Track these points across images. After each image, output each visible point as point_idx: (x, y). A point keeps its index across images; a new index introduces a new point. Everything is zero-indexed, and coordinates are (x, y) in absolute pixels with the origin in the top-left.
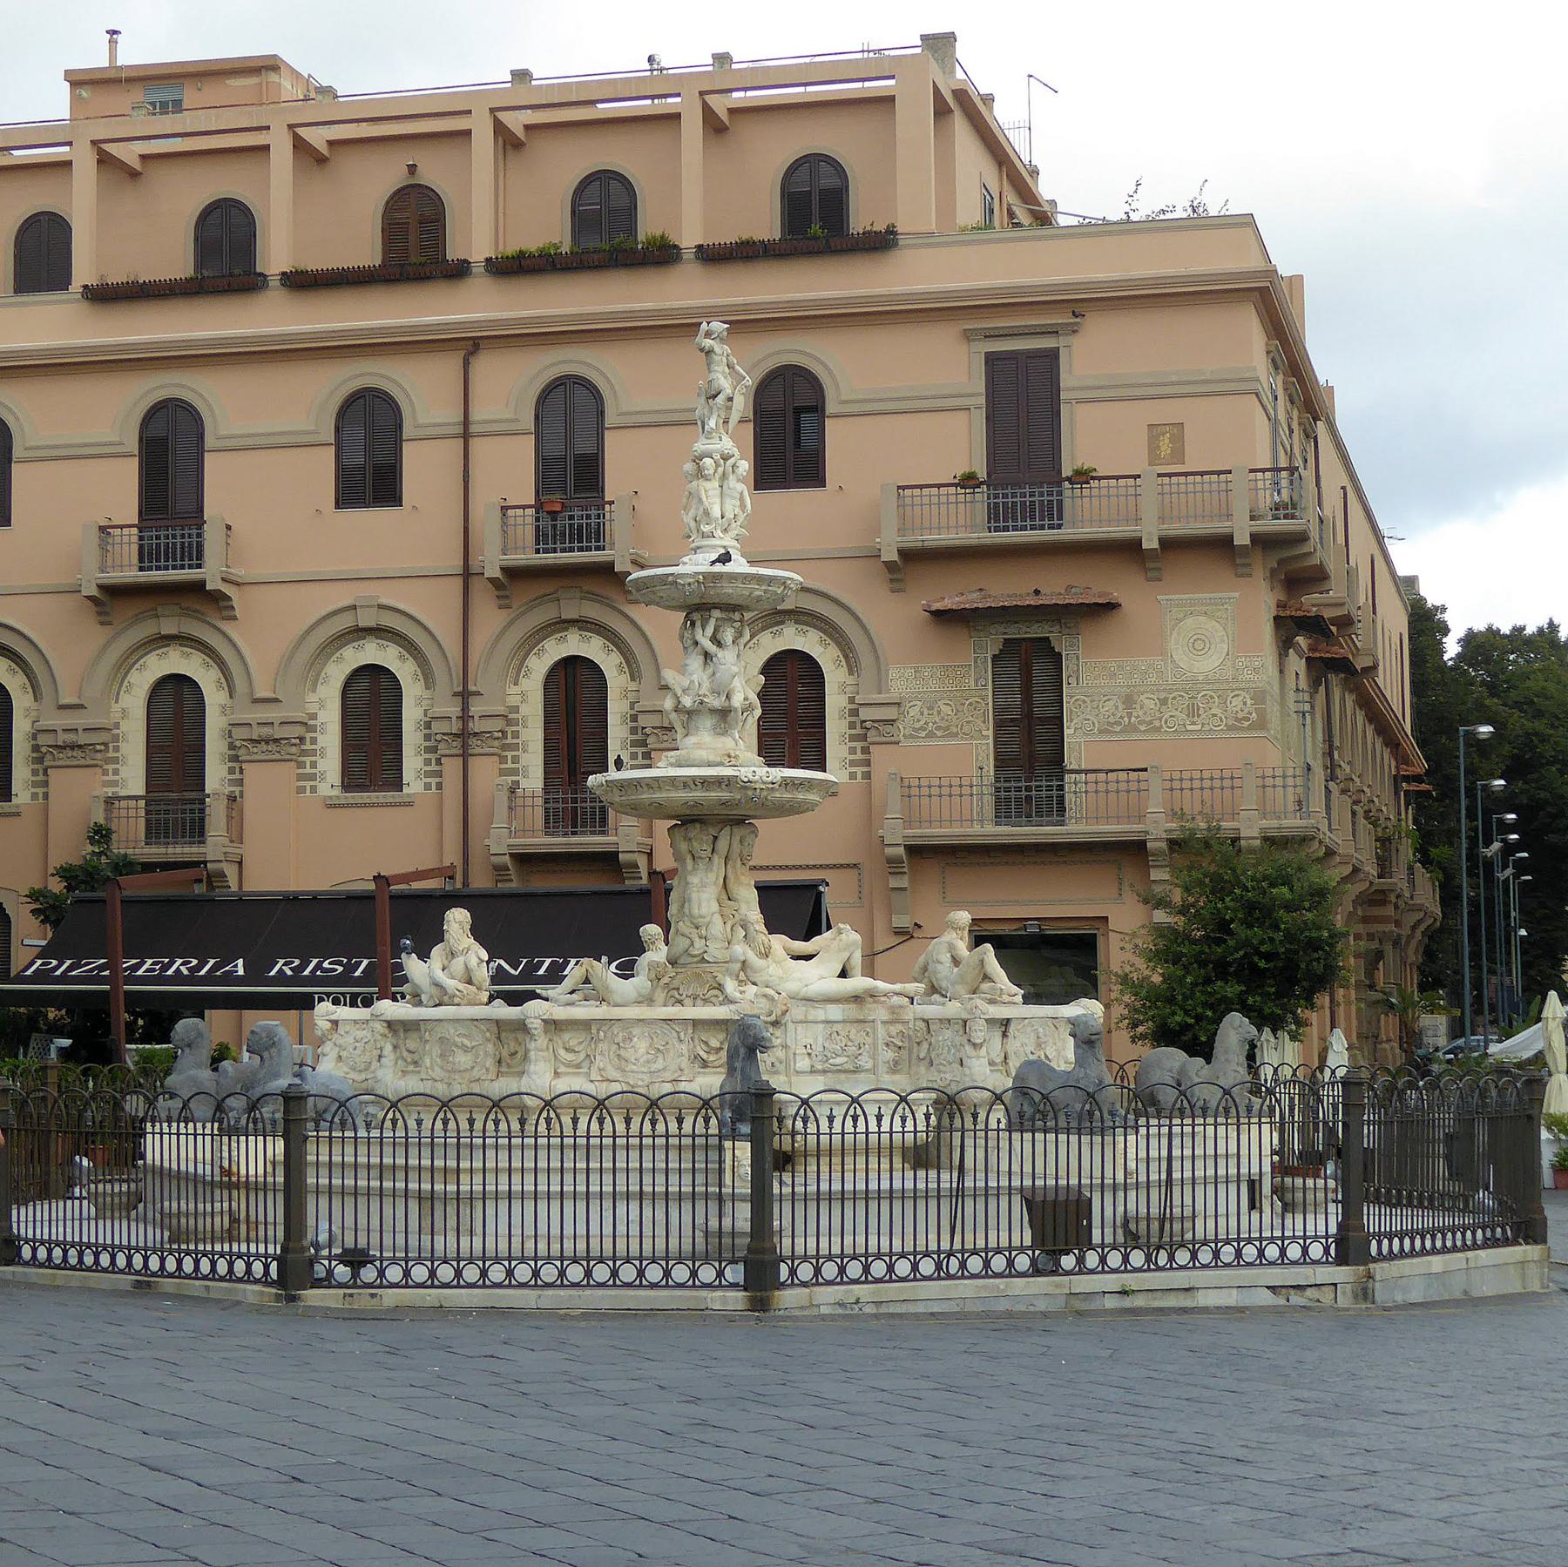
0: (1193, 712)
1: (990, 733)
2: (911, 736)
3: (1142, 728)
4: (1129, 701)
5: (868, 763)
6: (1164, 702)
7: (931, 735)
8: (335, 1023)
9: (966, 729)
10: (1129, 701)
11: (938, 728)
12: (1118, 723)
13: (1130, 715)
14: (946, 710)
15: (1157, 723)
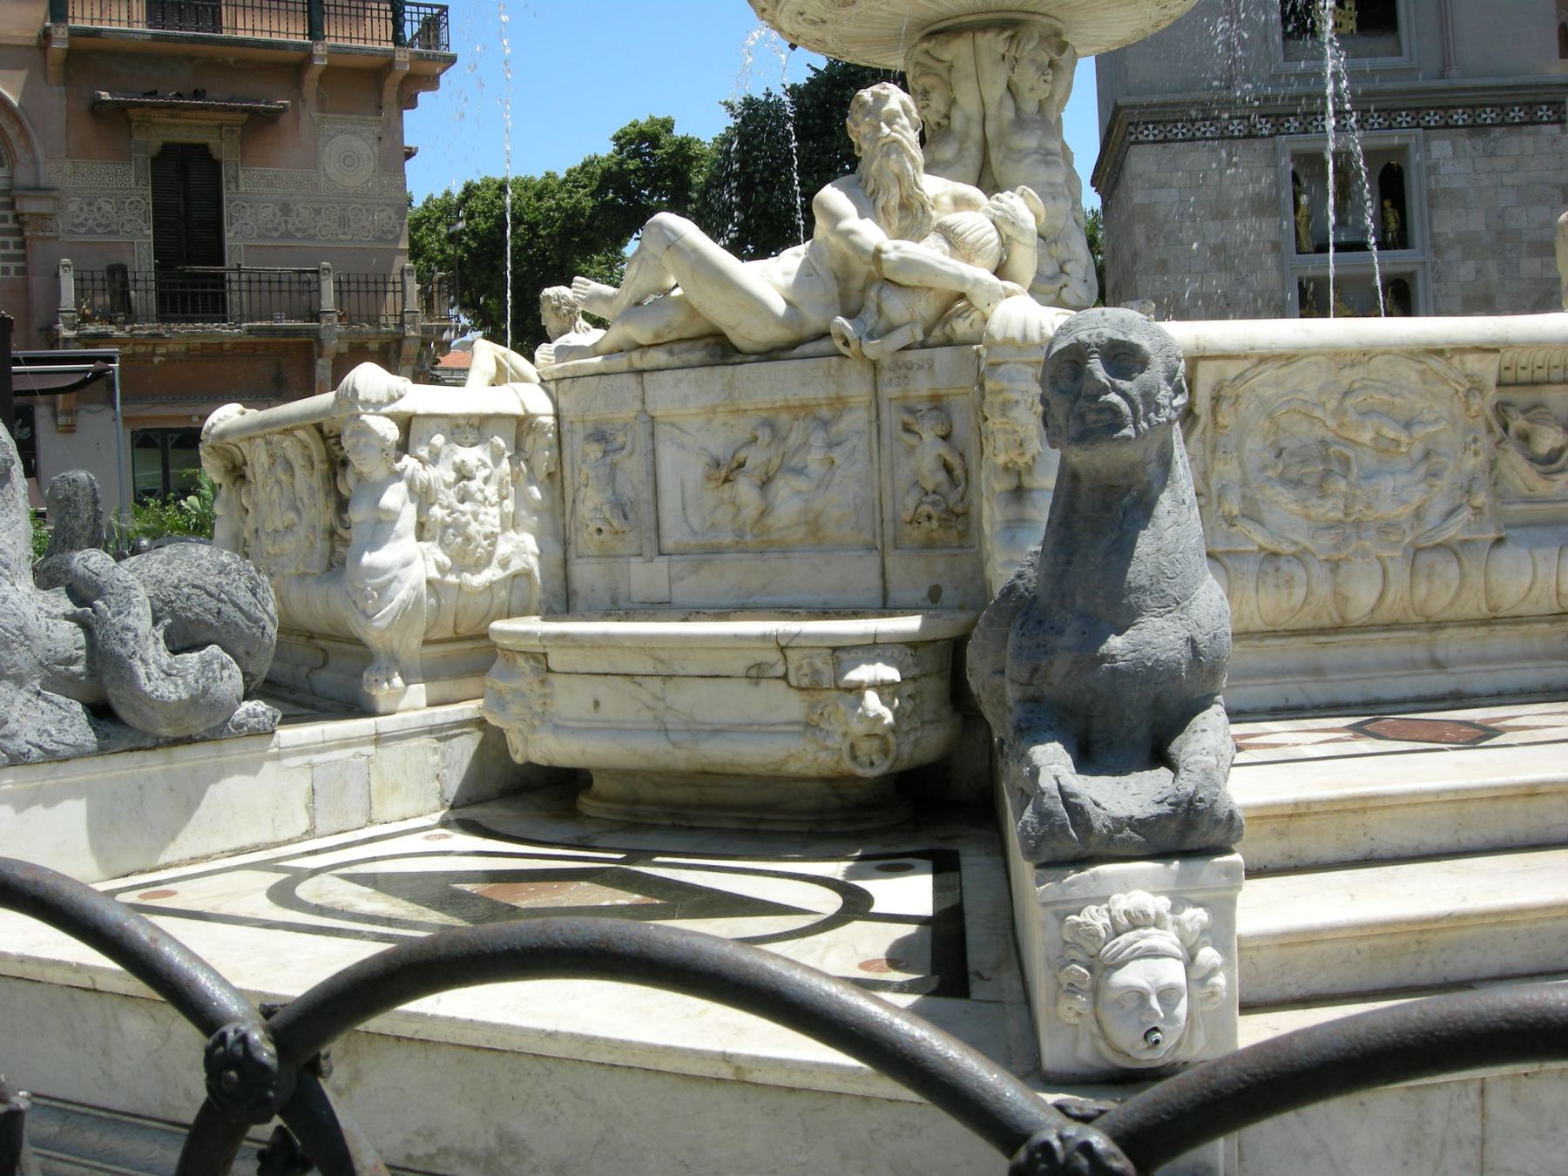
0: (344, 223)
1: (150, 232)
2: (70, 232)
3: (299, 235)
4: (286, 209)
5: (24, 258)
6: (318, 212)
7: (91, 231)
8: (406, 423)
9: (128, 227)
10: (286, 209)
11: (99, 225)
12: (276, 230)
13: (286, 222)
14: (108, 207)
15: (312, 232)
